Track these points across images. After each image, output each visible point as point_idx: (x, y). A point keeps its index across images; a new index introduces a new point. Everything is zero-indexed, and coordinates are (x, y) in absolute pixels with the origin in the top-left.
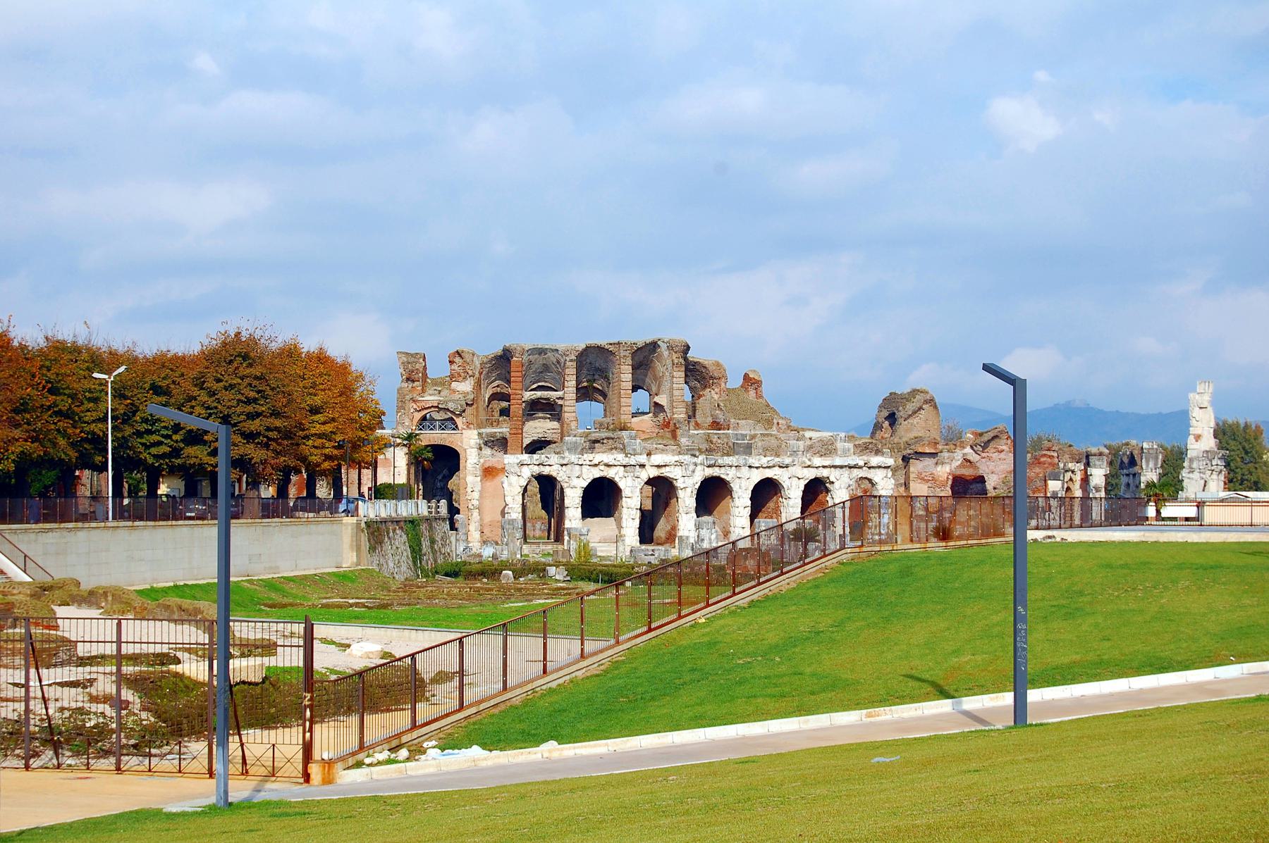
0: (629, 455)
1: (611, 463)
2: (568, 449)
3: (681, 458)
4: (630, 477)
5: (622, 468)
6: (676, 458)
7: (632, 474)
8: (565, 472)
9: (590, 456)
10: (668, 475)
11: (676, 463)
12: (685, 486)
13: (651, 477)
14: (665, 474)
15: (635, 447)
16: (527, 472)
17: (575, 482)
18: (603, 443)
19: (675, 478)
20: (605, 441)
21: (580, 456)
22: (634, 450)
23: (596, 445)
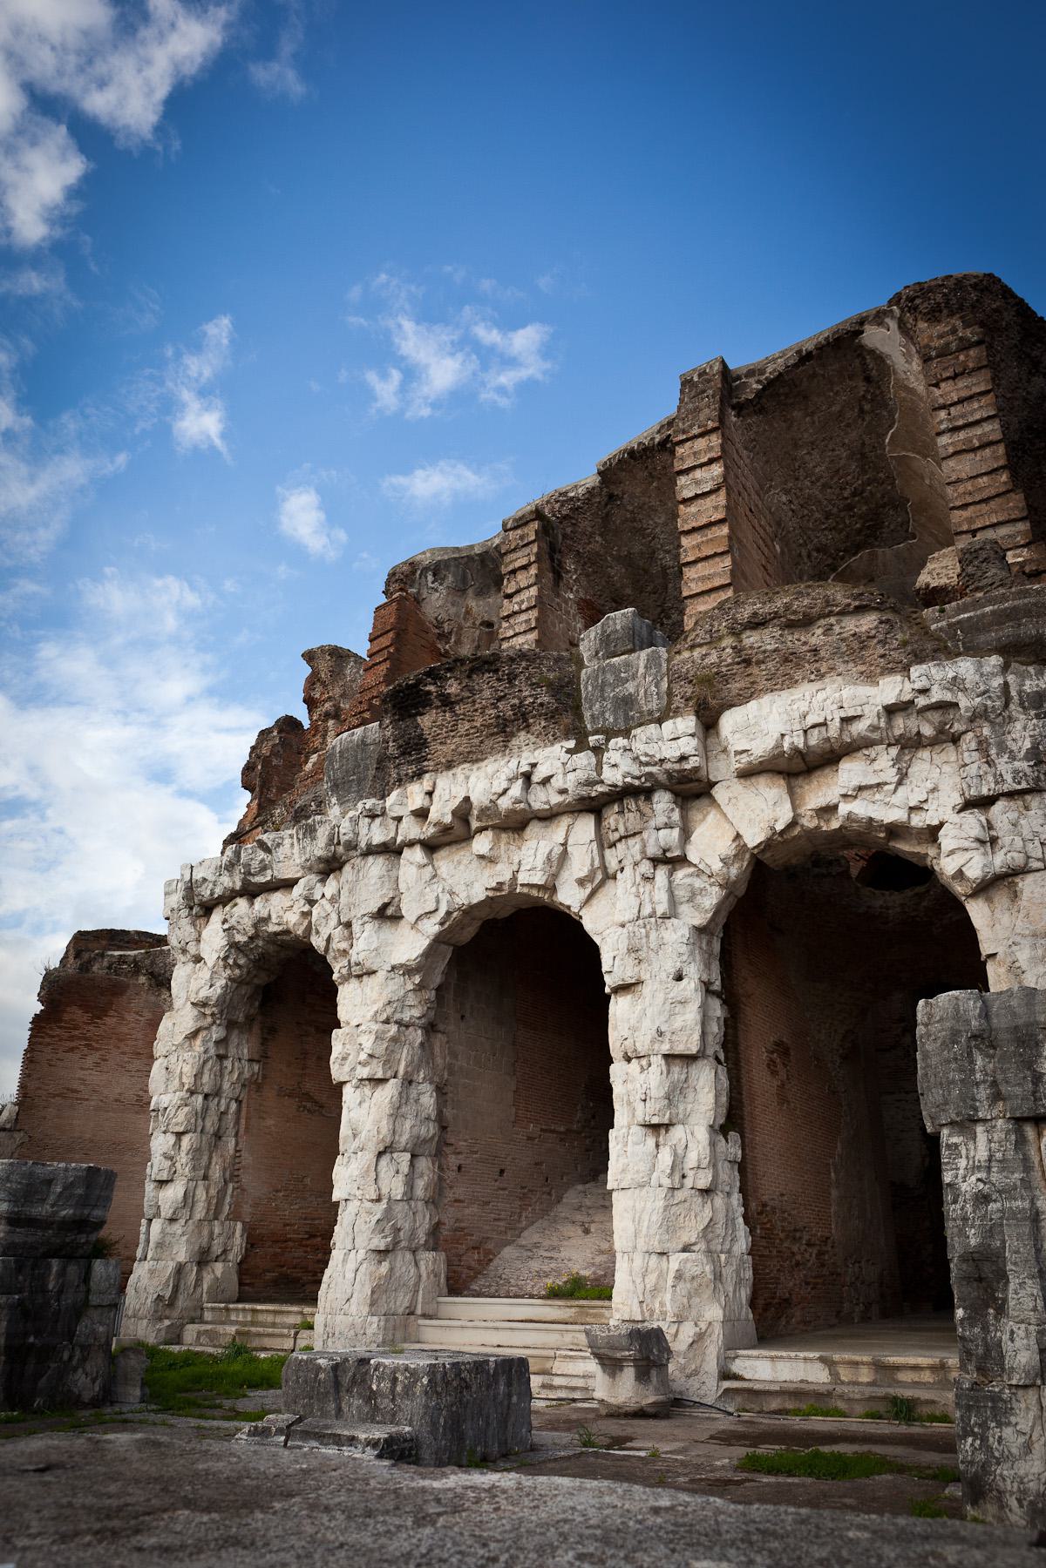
0: (592, 740)
1: (505, 803)
2: (335, 787)
3: (932, 678)
4: (628, 870)
5: (585, 827)
6: (891, 689)
7: (634, 845)
8: (334, 900)
9: (415, 795)
10: (861, 808)
11: (900, 725)
12: (999, 861)
13: (754, 838)
14: (844, 809)
15: (630, 687)
16: (213, 939)
17: (367, 942)
18: (447, 702)
19: (918, 821)
20: (453, 688)
21: (370, 803)
22: (628, 702)
23: (426, 721)
